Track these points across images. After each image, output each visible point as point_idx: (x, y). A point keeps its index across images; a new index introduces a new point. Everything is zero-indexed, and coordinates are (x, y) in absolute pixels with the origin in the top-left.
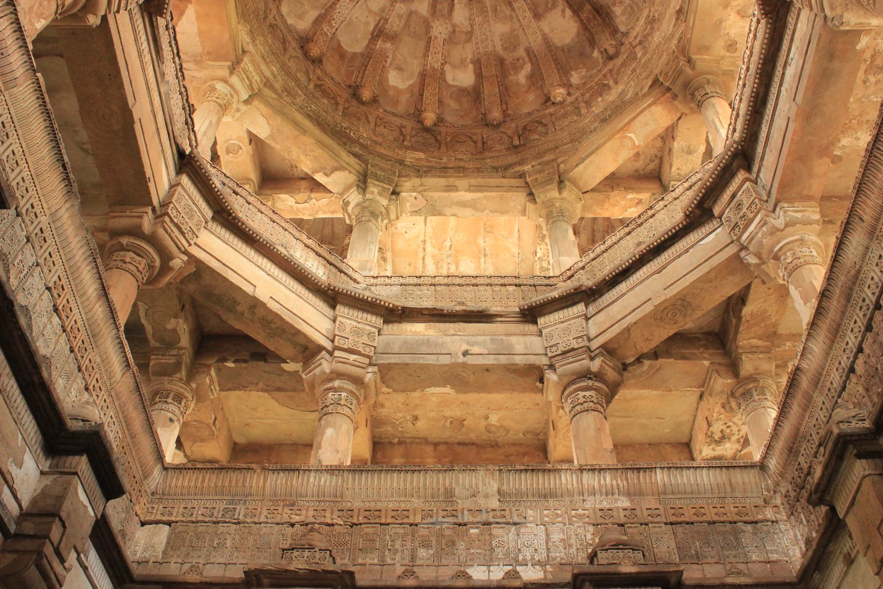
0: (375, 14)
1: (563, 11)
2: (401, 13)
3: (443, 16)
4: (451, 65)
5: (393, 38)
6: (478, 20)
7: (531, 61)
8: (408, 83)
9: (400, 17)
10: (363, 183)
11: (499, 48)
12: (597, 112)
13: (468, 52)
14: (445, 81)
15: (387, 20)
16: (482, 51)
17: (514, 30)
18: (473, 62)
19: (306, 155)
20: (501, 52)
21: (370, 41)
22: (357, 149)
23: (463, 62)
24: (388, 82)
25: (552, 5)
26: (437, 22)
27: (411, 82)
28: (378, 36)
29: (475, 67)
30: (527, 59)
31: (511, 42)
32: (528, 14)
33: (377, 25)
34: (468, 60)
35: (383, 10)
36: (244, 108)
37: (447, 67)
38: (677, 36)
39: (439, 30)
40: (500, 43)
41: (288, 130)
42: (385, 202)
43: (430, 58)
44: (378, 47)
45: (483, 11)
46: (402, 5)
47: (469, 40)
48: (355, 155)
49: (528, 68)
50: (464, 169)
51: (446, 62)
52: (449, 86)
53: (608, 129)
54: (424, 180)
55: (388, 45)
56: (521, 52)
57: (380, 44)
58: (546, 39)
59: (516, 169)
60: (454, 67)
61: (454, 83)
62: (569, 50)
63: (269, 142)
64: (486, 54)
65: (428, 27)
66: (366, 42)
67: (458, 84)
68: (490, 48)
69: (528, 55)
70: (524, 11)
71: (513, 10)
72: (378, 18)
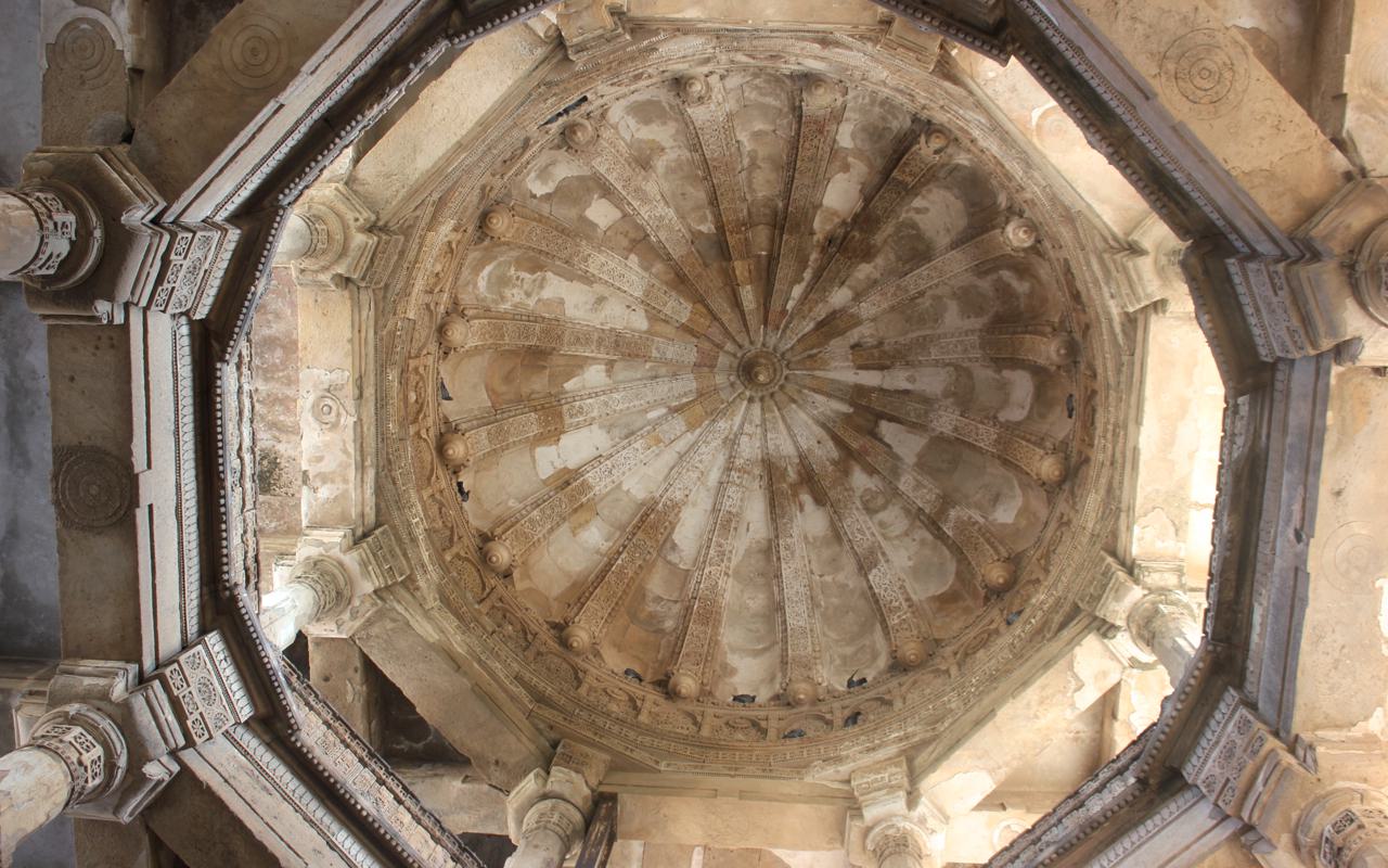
0: (911, 525)
1: (918, 211)
2: (913, 483)
3: (926, 412)
4: (1001, 407)
5: (946, 501)
6: (934, 353)
7: (996, 269)
8: (1018, 491)
9: (919, 485)
10: (1106, 629)
11: (977, 323)
12: (1021, 173)
13: (984, 374)
14: (1019, 424)
15: (920, 509)
16: (978, 354)
17: (954, 294)
18: (999, 371)
19: (1036, 717)
20: (985, 319)
21: (946, 544)
22: (1058, 619)
23: (1003, 387)
24: (1004, 525)
25: (913, 228)
26: (934, 424)
27: (1016, 483)
28: (939, 529)
29: (1006, 368)
30: (995, 276)
31: (969, 301)
32: (923, 270)
33: (926, 526)
34: (997, 377)
35: (907, 512)
36: (923, 808)
37: (1002, 417)
38: (859, 44)
39: (946, 421)
40: (972, 320)
41: (984, 738)
42: (1136, 593)
43: (982, 445)
44: (950, 533)
45: (923, 344)
46: (903, 480)
47: (969, 374)
48: (1063, 626)
49: (1006, 275)
50: (1116, 426)
51: (995, 417)
52: (1029, 417)
53: (1036, 159)
54: (1124, 506)
55: (953, 513)
56: (985, 285)
57: (948, 530)
58: (954, 245)
59: (1118, 329)
60: (1005, 403)
61: (1027, 408)
62: (973, 205)
63: (1002, 774)
64: (982, 347)
65: (939, 441)
66: (946, 552)
67: (1029, 400)
68: (975, 338)
69: (986, 273)
70: (920, 276)
71: (921, 294)
72: (918, 523)
